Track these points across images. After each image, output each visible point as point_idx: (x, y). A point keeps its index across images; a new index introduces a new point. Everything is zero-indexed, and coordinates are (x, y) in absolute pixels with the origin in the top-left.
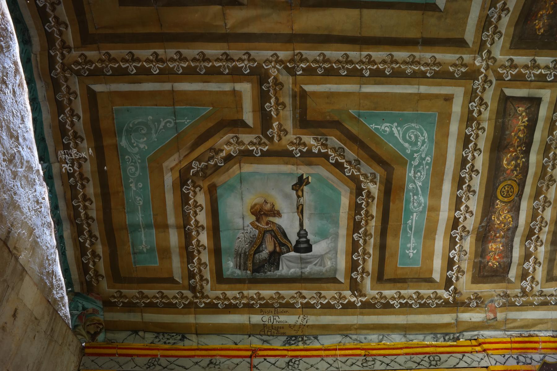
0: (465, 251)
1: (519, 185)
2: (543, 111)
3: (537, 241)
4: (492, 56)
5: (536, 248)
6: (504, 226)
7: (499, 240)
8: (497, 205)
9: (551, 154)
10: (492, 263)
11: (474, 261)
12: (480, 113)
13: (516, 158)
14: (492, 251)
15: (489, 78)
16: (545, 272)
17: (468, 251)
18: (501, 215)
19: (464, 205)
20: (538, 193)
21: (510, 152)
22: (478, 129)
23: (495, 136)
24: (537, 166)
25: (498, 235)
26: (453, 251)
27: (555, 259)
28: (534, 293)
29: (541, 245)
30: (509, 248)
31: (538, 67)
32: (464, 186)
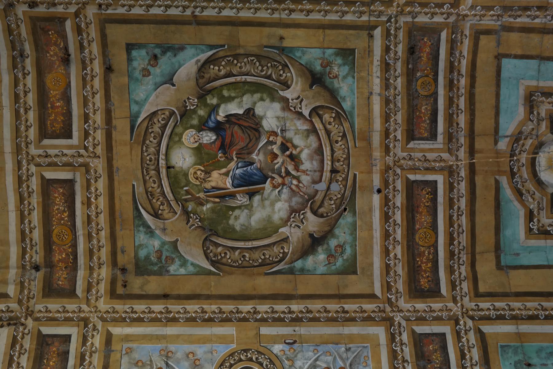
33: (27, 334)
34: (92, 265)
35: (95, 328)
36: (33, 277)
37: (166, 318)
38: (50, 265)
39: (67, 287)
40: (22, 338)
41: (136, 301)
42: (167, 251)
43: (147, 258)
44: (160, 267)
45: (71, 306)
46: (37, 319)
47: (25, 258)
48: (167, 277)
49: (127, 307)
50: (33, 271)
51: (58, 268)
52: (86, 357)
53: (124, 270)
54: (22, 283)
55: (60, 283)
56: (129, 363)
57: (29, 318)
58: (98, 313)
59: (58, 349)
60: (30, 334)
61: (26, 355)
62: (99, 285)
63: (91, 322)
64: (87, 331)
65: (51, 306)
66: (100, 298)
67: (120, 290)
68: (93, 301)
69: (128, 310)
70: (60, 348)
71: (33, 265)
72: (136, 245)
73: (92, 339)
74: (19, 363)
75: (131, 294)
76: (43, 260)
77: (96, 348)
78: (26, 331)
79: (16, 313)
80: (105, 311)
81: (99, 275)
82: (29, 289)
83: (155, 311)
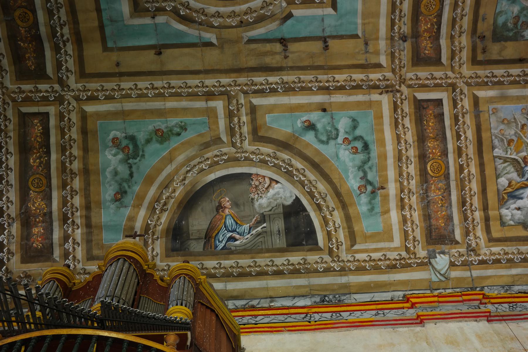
0: (13, 235)
1: (46, 178)
2: (52, 122)
3: (73, 225)
4: (4, 86)
5: (73, 231)
6: (40, 212)
7: (40, 224)
8: (31, 194)
9: (67, 153)
10: (36, 244)
11: (21, 244)
12: (6, 126)
13: (40, 157)
14: (35, 234)
15: (6, 101)
16: (85, 251)
17: (15, 235)
18: (36, 203)
19: (5, 197)
20: (64, 185)
21: (35, 153)
22: (6, 137)
23: (20, 143)
24: (57, 162)
25: (37, 220)
26: (3, 236)
27: (92, 241)
28: (78, 271)
29: (78, 228)
30: (49, 230)
31: (41, 91)
32: (3, 182)
33: (405, 100)
34: (453, 34)
35: (462, 93)
36: (402, 48)
37: (524, 80)
38: (416, 35)
39: (433, 56)
40: (402, 103)
41: (495, 66)
42: (525, 16)
43: (505, 24)
44: (515, 33)
45: (438, 74)
46: (409, 86)
47: (394, 29)
48: (522, 42)
49: (487, 72)
50: (401, 42)
51: (423, 38)
52: (460, 118)
53: (482, 38)
54: (392, 55)
55: (427, 52)
56: (497, 121)
57: (402, 85)
58: (463, 79)
59: (434, 112)
60: (407, 100)
61: (408, 117)
62: (462, 53)
63: (458, 87)
64: (455, 95)
65: (421, 74)
66: (463, 64)
67: (480, 57)
68: (457, 68)
69: (489, 75)
70: (435, 111)
71: (401, 36)
72: (497, 11)
73: (461, 101)
74: (403, 125)
75: (490, 60)
76: (410, 31)
77: (467, 110)
78: (403, 97)
79: (391, 82)
80: (469, 76)
81: (460, 43)
82: (399, 59)
83: (514, 74)
